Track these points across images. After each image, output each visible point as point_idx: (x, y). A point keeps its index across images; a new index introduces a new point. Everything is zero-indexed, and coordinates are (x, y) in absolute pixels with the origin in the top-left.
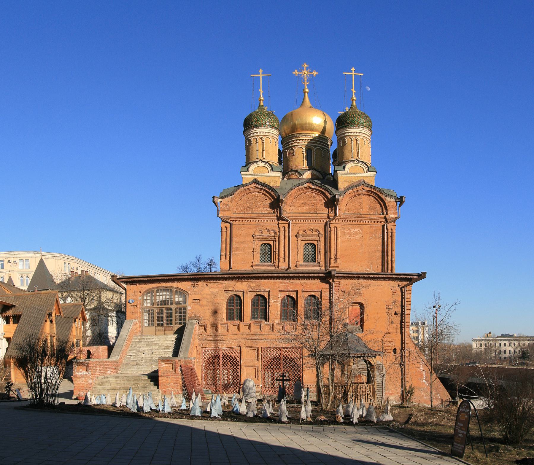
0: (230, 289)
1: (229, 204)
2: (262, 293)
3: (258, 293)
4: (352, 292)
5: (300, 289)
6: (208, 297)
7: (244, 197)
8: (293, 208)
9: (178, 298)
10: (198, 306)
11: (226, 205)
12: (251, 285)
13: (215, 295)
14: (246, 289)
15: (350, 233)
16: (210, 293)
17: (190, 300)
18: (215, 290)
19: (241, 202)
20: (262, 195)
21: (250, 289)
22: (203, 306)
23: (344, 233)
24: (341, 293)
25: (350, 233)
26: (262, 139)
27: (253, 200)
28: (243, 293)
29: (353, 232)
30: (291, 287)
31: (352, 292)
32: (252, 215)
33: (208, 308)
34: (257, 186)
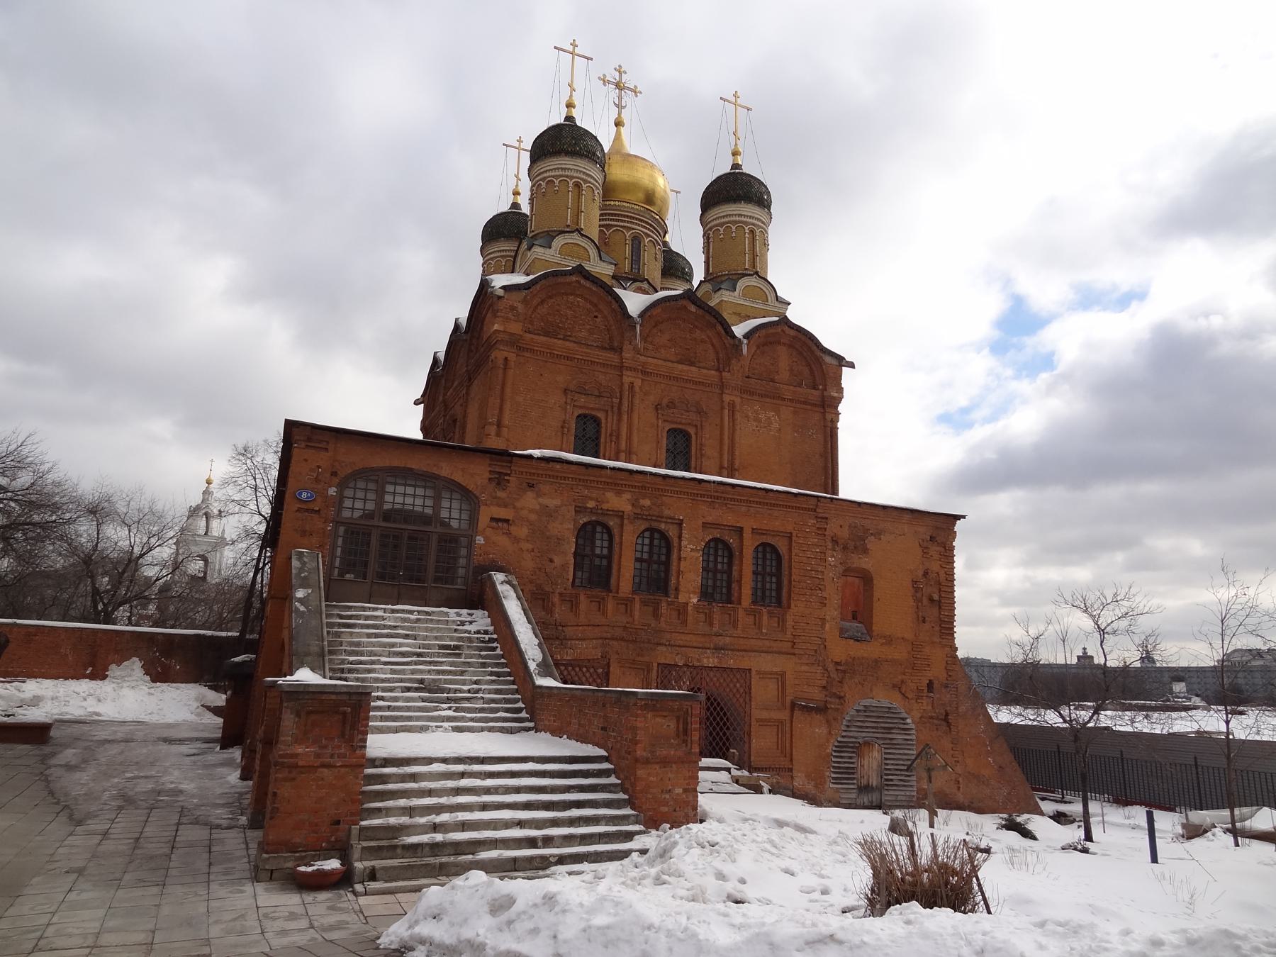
0: (591, 504)
1: (520, 307)
2: (663, 526)
3: (655, 525)
4: (851, 544)
5: (748, 524)
6: (533, 517)
8: (651, 347)
9: (453, 513)
10: (503, 541)
11: (513, 308)
12: (642, 502)
13: (548, 514)
14: (628, 508)
15: (757, 420)
16: (538, 507)
17: (484, 520)
18: (552, 502)
19: (543, 310)
20: (589, 306)
21: (638, 511)
22: (517, 540)
23: (747, 417)
24: (830, 545)
25: (757, 420)
26: (577, 185)
27: (569, 312)
28: (622, 517)
29: (762, 416)
30: (730, 519)
31: (851, 544)
32: (568, 344)
33: (530, 546)
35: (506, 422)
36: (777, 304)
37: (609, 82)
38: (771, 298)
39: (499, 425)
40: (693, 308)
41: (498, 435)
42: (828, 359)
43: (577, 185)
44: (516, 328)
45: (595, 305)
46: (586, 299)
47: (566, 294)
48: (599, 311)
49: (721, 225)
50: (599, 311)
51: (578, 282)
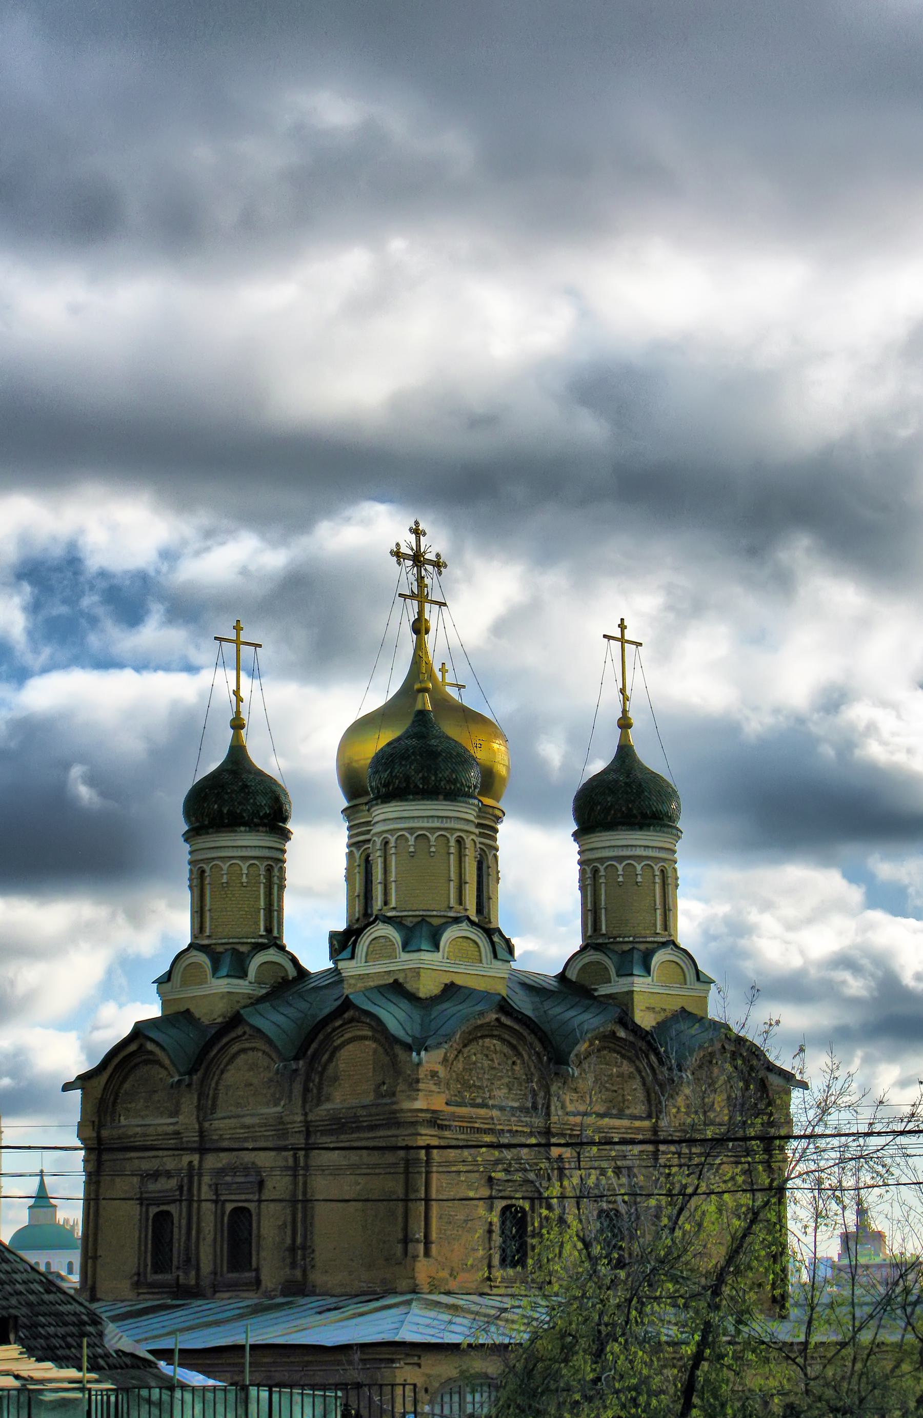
7: (466, 1050)
20: (506, 1049)
26: (460, 842)
34: (504, 1019)
35: (434, 1236)
36: (698, 986)
37: (406, 557)
38: (690, 975)
39: (427, 1242)
40: (622, 1034)
41: (427, 1254)
42: (774, 1080)
43: (460, 842)
44: (438, 1103)
45: (514, 1047)
46: (503, 1040)
47: (482, 1037)
48: (519, 1055)
49: (620, 859)
50: (519, 1055)
51: (498, 1020)
